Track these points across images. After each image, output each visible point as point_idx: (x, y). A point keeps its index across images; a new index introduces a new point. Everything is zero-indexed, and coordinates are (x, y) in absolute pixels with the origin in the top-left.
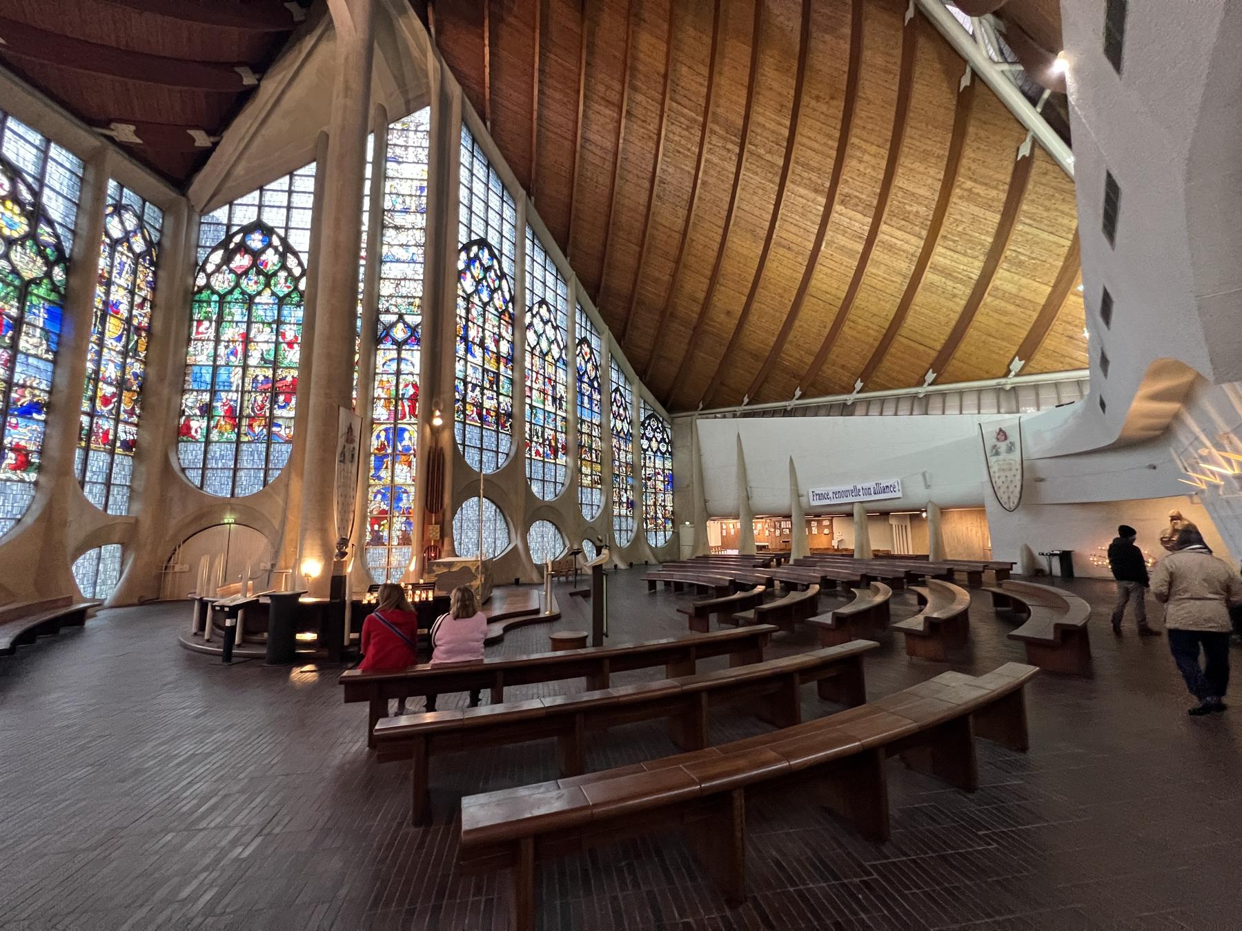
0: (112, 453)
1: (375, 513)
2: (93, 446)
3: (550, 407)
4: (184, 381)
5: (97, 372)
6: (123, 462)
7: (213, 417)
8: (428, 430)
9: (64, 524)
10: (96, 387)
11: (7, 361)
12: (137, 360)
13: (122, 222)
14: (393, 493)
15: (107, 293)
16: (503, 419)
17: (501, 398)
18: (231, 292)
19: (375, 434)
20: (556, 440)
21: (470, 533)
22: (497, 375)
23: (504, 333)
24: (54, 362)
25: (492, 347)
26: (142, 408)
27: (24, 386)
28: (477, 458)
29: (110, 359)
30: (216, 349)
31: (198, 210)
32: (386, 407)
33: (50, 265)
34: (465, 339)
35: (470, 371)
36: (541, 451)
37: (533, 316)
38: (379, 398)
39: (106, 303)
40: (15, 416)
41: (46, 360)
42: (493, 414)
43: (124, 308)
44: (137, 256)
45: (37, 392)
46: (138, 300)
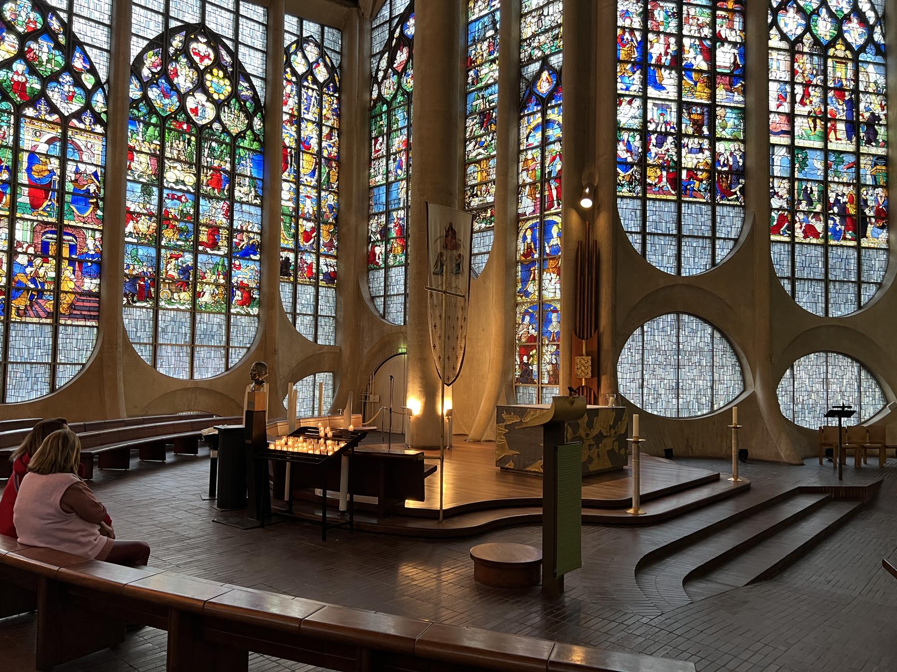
0: (317, 286)
1: (523, 340)
2: (300, 280)
3: (840, 142)
4: (370, 205)
5: (297, 209)
6: (327, 295)
7: (389, 240)
8: (574, 218)
9: (275, 352)
10: (297, 224)
11: (227, 211)
12: (331, 192)
13: (305, 57)
14: (542, 310)
15: (299, 131)
16: (718, 181)
17: (720, 147)
18: (395, 97)
19: (521, 234)
20: (860, 203)
21: (659, 371)
23: (724, 32)
24: (261, 206)
26: (338, 240)
27: (241, 231)
28: (671, 251)
29: (304, 193)
30: (387, 165)
31: (368, 17)
32: (531, 195)
33: (250, 117)
34: (643, 64)
35: (653, 113)
36: (819, 227)
38: (524, 185)
39: (298, 141)
40: (238, 258)
41: (255, 205)
42: (702, 175)
43: (314, 142)
44: (321, 86)
45: (251, 235)
46: (326, 131)
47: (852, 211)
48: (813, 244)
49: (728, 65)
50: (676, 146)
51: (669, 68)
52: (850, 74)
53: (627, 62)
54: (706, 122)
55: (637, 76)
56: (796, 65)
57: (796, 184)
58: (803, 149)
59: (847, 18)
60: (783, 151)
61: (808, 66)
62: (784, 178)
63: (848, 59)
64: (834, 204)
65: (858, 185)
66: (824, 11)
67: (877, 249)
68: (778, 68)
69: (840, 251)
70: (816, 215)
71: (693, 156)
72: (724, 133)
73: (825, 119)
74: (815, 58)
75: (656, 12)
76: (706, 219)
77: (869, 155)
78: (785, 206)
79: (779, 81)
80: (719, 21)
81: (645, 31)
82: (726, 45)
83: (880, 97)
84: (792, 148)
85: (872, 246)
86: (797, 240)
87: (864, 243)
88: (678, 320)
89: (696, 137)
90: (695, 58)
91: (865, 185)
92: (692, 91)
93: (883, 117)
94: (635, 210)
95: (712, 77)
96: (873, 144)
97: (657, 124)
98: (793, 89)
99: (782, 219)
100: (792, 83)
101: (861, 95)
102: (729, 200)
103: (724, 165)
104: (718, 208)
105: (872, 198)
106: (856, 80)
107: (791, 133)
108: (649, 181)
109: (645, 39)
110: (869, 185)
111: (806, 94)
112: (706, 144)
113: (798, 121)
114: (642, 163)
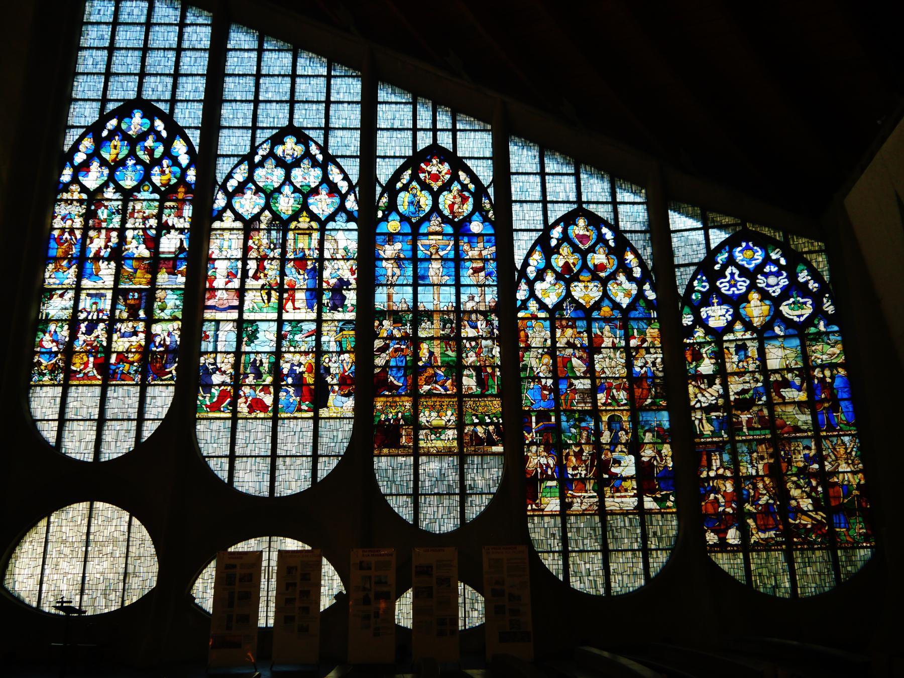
3: (299, 310)
17: (156, 328)
20: (320, 371)
22: (149, 295)
23: (172, 220)
25: (143, 251)
35: (85, 303)
36: (268, 400)
37: (253, 168)
47: (310, 379)
48: (260, 419)
49: (173, 250)
51: (108, 259)
52: (315, 244)
53: (64, 259)
54: (143, 305)
55: (73, 270)
56: (250, 243)
57: (243, 358)
58: (253, 322)
59: (315, 191)
60: (230, 326)
61: (265, 241)
62: (228, 353)
63: (313, 229)
64: (288, 376)
66: (287, 189)
67: (340, 418)
68: (230, 247)
69: (293, 423)
70: (265, 389)
71: (125, 339)
72: (162, 315)
73: (282, 292)
74: (274, 233)
75: (99, 212)
76: (135, 401)
77: (333, 321)
78: (228, 380)
79: (229, 259)
80: (167, 211)
81: (86, 229)
82: (173, 231)
83: (351, 262)
84: (240, 323)
85: (335, 415)
86: (240, 415)
87: (323, 412)
88: (91, 508)
89: (130, 321)
90: (137, 248)
91: (328, 352)
92: (131, 278)
93: (353, 282)
94: (54, 398)
95: (155, 263)
96: (340, 309)
98: (245, 264)
99: (223, 396)
100: (245, 259)
101: (326, 263)
102: (162, 380)
103: (160, 345)
104: (150, 389)
105: (336, 365)
106: (321, 249)
107: (240, 308)
108: (73, 368)
109: (85, 236)
111: (261, 268)
112: (141, 326)
113: (249, 296)
114: (68, 351)
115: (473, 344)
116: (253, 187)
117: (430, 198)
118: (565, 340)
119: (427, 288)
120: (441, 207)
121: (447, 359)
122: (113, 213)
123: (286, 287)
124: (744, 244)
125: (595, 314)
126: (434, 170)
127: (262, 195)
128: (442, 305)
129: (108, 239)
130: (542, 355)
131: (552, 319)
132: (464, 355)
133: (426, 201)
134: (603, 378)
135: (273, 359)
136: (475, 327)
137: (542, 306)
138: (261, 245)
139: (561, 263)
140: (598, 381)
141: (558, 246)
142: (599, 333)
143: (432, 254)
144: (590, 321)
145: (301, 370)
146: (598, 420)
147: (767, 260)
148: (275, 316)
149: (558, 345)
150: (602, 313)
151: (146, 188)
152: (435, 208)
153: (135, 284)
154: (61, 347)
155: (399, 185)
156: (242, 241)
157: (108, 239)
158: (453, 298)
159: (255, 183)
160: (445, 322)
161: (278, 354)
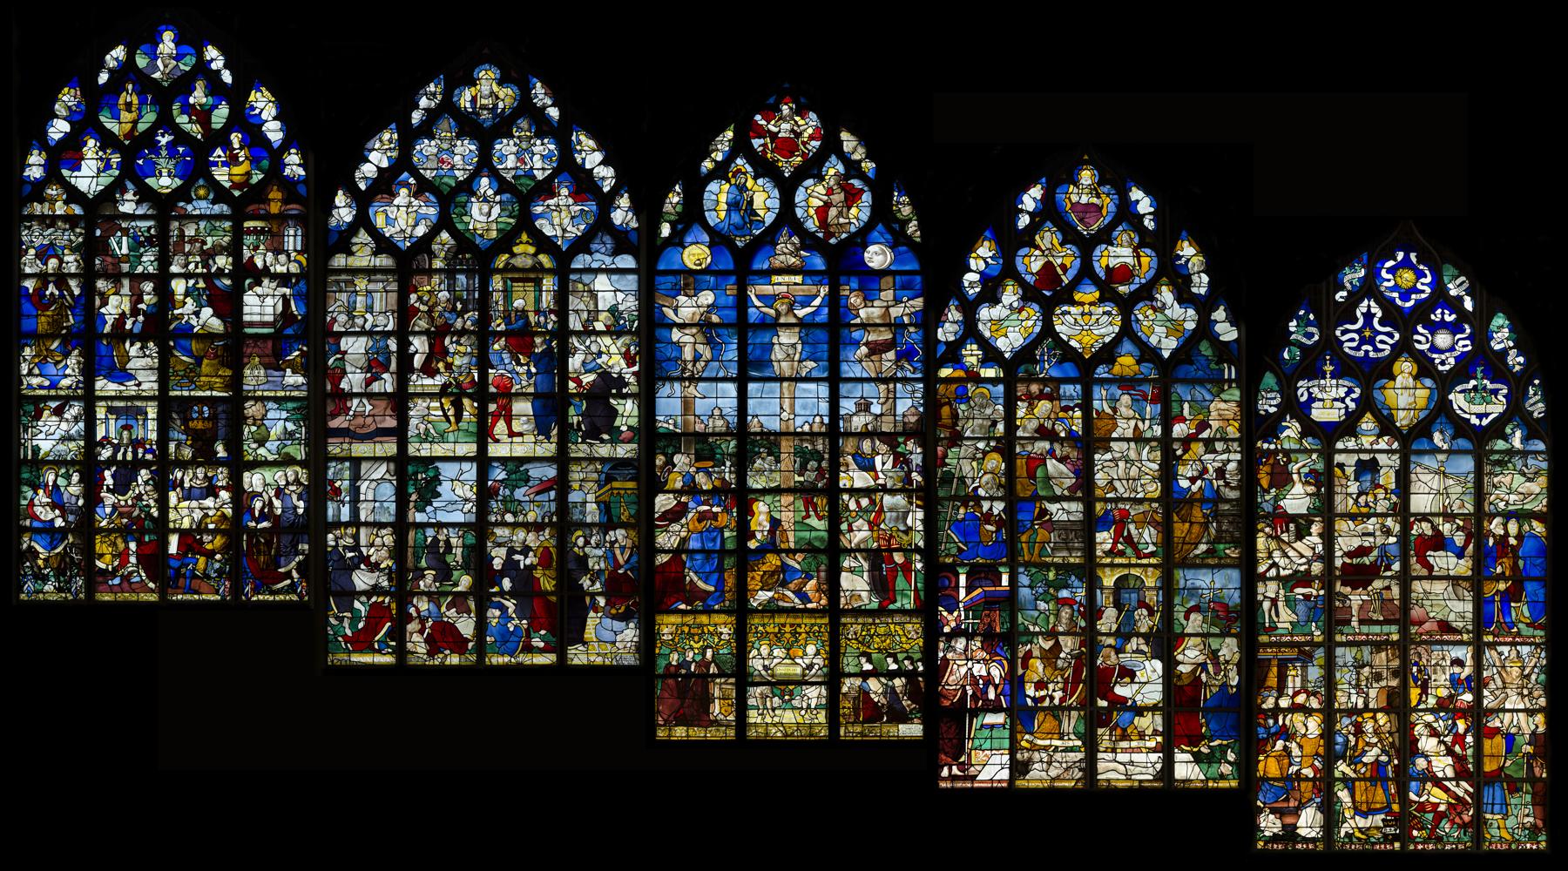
3: (519, 438)
20: (567, 565)
25: (208, 319)
42: (213, 543)
50: (156, 488)
51: (142, 338)
61: (444, 295)
64: (503, 573)
65: (563, 522)
71: (194, 504)
73: (483, 401)
74: (462, 278)
75: (113, 242)
89: (199, 465)
90: (197, 314)
91: (582, 525)
97: (116, 448)
98: (404, 344)
110: (592, 525)
111: (437, 352)
112: (222, 476)
113: (417, 409)
115: (865, 502)
116: (412, 181)
117: (776, 193)
118: (1034, 424)
119: (768, 385)
120: (799, 212)
121: (807, 535)
122: (141, 244)
123: (492, 389)
124: (1400, 256)
125: (1101, 371)
126: (785, 129)
127: (432, 198)
128: (799, 421)
129: (137, 297)
130: (985, 453)
131: (1009, 381)
132: (844, 527)
133: (765, 200)
134: (1111, 500)
135: (471, 539)
136: (868, 467)
137: (991, 355)
138: (437, 304)
139: (1036, 266)
140: (1099, 506)
141: (1034, 228)
142: (1109, 411)
143: (778, 314)
144: (1087, 381)
145: (528, 562)
146: (1093, 584)
147: (1440, 297)
148: (470, 449)
149: (1020, 433)
150: (1117, 369)
151: (202, 192)
152: (787, 216)
153: (200, 388)
154: (71, 518)
155: (707, 165)
156: (393, 297)
157: (137, 297)
158: (824, 407)
159: (414, 172)
160: (804, 457)
161: (480, 528)
